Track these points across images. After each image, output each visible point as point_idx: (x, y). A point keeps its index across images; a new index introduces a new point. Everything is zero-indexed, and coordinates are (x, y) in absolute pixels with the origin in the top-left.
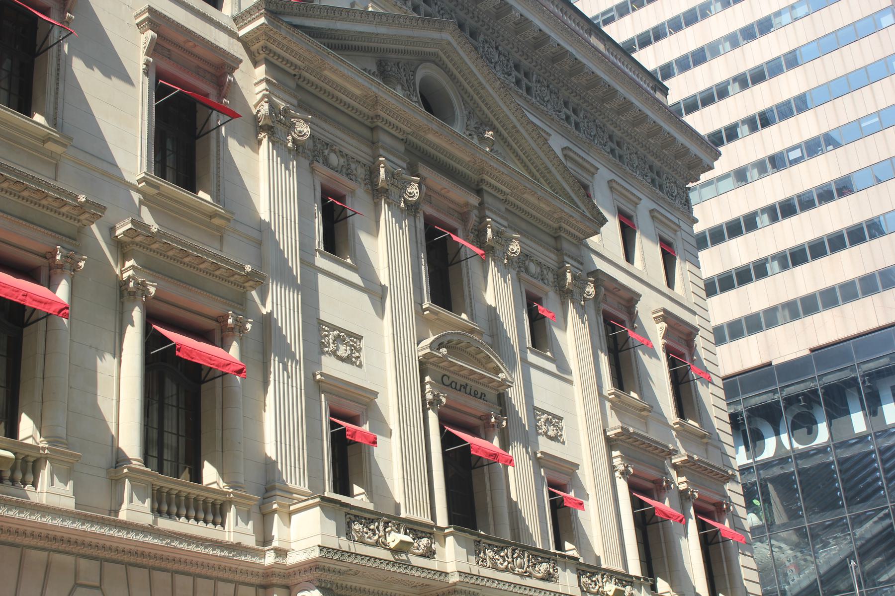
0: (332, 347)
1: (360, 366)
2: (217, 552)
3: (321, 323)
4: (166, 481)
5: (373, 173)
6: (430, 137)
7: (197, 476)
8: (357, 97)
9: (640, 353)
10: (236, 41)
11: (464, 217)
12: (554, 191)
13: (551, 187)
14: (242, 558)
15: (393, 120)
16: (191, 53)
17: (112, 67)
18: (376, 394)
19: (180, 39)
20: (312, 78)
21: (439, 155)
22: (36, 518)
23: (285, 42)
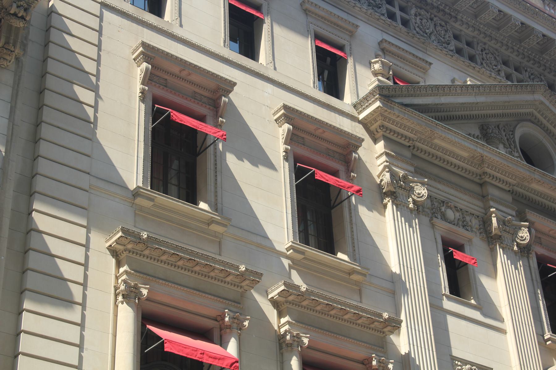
5: (486, 223)
6: (535, 186)
8: (465, 159)
10: (357, 124)
15: (499, 175)
17: (258, 157)
19: (311, 127)
20: (424, 147)
21: (544, 201)
23: (398, 119)
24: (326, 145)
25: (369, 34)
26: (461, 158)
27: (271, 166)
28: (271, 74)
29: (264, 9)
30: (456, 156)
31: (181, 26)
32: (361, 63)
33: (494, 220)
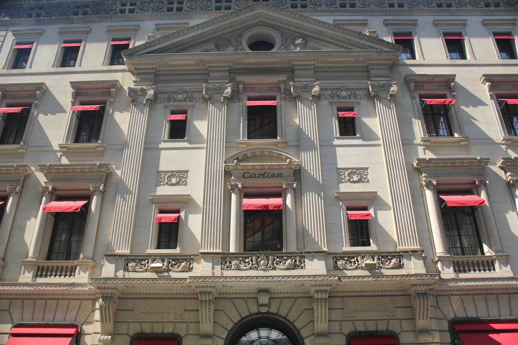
0: (347, 178)
1: (368, 181)
2: (62, 288)
3: (338, 169)
4: (54, 263)
6: (246, 61)
7: (482, 252)
8: (194, 65)
9: (463, 108)
11: (279, 89)
12: (361, 48)
13: (359, 48)
14: (76, 289)
15: (218, 64)
16: (97, 89)
17: (477, 102)
18: (376, 193)
19: (89, 86)
20: (166, 68)
21: (259, 66)
22: (21, 288)
24: (101, 90)
25: (474, 21)
26: (191, 65)
27: (483, 104)
28: (426, 62)
29: (463, 34)
30: (189, 65)
31: (424, 59)
32: (423, 37)
33: (370, 87)
